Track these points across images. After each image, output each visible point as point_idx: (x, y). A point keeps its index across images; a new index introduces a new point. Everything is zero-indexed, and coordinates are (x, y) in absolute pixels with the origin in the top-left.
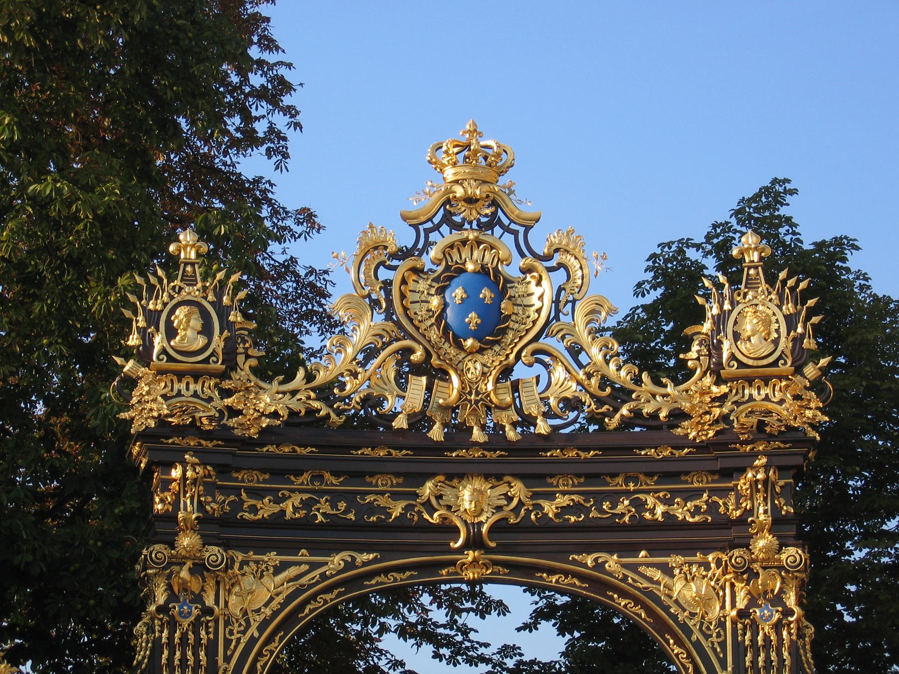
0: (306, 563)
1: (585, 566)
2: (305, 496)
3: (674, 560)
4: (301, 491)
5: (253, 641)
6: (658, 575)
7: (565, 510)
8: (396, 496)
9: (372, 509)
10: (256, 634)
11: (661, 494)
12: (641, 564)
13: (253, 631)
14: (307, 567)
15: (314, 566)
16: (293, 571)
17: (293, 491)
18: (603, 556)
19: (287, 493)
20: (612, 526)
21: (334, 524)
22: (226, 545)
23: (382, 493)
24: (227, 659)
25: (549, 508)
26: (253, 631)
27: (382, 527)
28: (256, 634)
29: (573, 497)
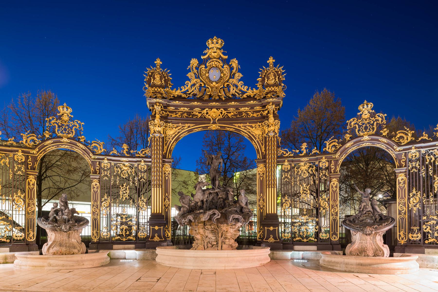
1: (236, 126)
3: (253, 125)
7: (232, 115)
8: (199, 113)
13: (171, 139)
15: (183, 127)
16: (179, 128)
17: (179, 112)
18: (240, 125)
22: (166, 122)
26: (171, 139)
27: (197, 119)
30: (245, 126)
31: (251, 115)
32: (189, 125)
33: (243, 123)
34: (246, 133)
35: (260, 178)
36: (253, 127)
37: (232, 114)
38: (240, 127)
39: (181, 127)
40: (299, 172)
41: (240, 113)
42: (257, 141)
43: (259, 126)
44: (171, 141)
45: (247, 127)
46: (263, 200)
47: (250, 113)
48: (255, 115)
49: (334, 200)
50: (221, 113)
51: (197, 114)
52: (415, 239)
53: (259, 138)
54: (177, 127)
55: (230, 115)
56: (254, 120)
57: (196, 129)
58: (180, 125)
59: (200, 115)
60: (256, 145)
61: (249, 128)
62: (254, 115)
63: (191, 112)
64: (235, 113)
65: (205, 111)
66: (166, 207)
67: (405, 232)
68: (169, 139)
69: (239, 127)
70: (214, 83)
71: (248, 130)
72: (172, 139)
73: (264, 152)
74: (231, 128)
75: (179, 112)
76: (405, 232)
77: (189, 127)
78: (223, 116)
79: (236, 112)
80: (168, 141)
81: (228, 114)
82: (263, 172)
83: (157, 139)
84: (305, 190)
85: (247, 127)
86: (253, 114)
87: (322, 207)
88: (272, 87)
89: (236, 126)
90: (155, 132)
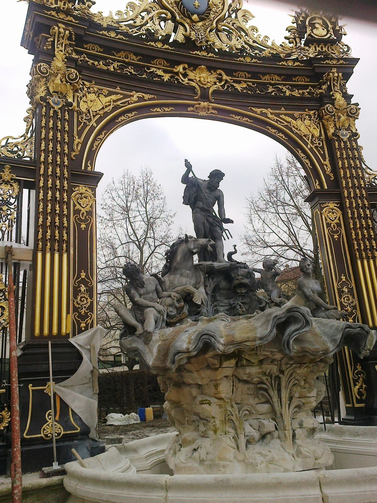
0: (121, 94)
1: (256, 113)
2: (119, 64)
3: (296, 114)
6: (289, 119)
8: (165, 71)
10: (95, 125)
11: (287, 87)
14: (122, 96)
15: (126, 96)
16: (114, 97)
17: (114, 60)
18: (264, 111)
19: (111, 61)
20: (268, 96)
23: (159, 69)
24: (80, 134)
25: (238, 87)
26: (93, 122)
28: (95, 125)
29: (249, 83)
30: (278, 115)
32: (140, 94)
33: (272, 109)
34: (280, 131)
36: (295, 119)
37: (245, 85)
38: (265, 115)
39: (119, 96)
41: (265, 86)
42: (311, 149)
43: (310, 116)
44: (93, 128)
45: (283, 116)
46: (351, 291)
47: (284, 88)
48: (296, 93)
50: (220, 80)
51: (160, 73)
53: (312, 143)
54: (110, 93)
55: (238, 87)
56: (294, 104)
57: (158, 110)
58: (118, 90)
60: (308, 157)
62: (293, 93)
63: (144, 66)
64: (251, 84)
65: (180, 68)
66: (80, 316)
68: (90, 120)
69: (262, 114)
70: (195, 17)
71: (286, 124)
72: (98, 122)
73: (332, 175)
75: (114, 60)
77: (141, 99)
78: (223, 86)
79: (253, 84)
80: (85, 125)
81: (235, 85)
83: (55, 112)
85: (283, 116)
89: (256, 113)
90: (49, 93)
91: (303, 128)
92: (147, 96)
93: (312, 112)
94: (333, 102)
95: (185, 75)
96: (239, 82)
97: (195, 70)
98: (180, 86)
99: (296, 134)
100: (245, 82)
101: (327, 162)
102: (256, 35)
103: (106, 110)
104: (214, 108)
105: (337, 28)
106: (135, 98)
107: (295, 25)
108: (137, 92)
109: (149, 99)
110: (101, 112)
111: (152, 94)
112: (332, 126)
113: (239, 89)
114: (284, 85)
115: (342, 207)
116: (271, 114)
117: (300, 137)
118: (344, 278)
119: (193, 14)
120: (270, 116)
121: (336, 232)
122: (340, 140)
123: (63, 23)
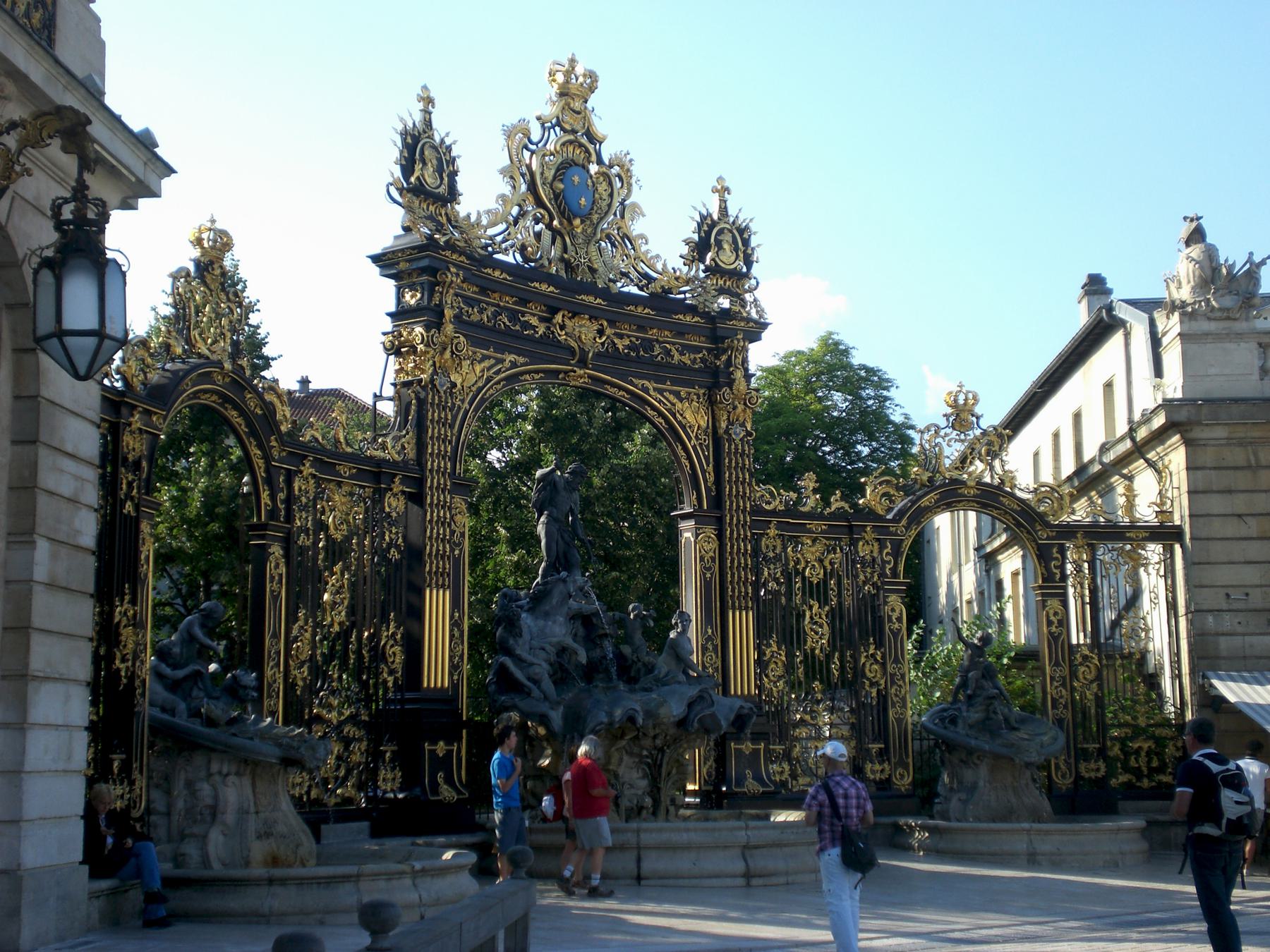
4: (493, 305)
5: (467, 412)
9: (527, 325)
12: (666, 390)
13: (466, 405)
16: (486, 364)
18: (647, 383)
21: (507, 332)
23: (534, 315)
27: (530, 339)
30: (661, 392)
31: (677, 356)
32: (512, 357)
34: (661, 414)
35: (704, 574)
36: (681, 400)
38: (646, 390)
40: (797, 562)
41: (648, 345)
42: (694, 447)
44: (467, 412)
48: (686, 359)
49: (896, 661)
51: (534, 321)
52: (1093, 775)
54: (485, 358)
59: (541, 330)
60: (689, 458)
61: (671, 397)
67: (1069, 756)
68: (463, 401)
74: (620, 388)
75: (488, 303)
76: (1069, 756)
77: (514, 365)
78: (603, 344)
80: (459, 408)
82: (711, 554)
84: (816, 623)
86: (682, 354)
87: (868, 679)
88: (726, 277)
89: (636, 386)
91: (688, 415)
92: (521, 360)
93: (702, 391)
94: (730, 383)
95: (562, 327)
96: (621, 336)
97: (573, 317)
98: (558, 345)
99: (680, 423)
100: (629, 336)
101: (711, 468)
102: (644, 248)
103: (480, 384)
104: (590, 377)
105: (749, 251)
106: (507, 364)
107: (696, 237)
108: (510, 353)
109: (522, 365)
110: (474, 389)
111: (524, 356)
112: (725, 417)
113: (621, 347)
114: (674, 344)
115: (720, 536)
116: (655, 389)
117: (683, 427)
118: (710, 631)
119: (575, 217)
120: (652, 392)
121: (709, 569)
122: (730, 440)
123: (455, 265)
